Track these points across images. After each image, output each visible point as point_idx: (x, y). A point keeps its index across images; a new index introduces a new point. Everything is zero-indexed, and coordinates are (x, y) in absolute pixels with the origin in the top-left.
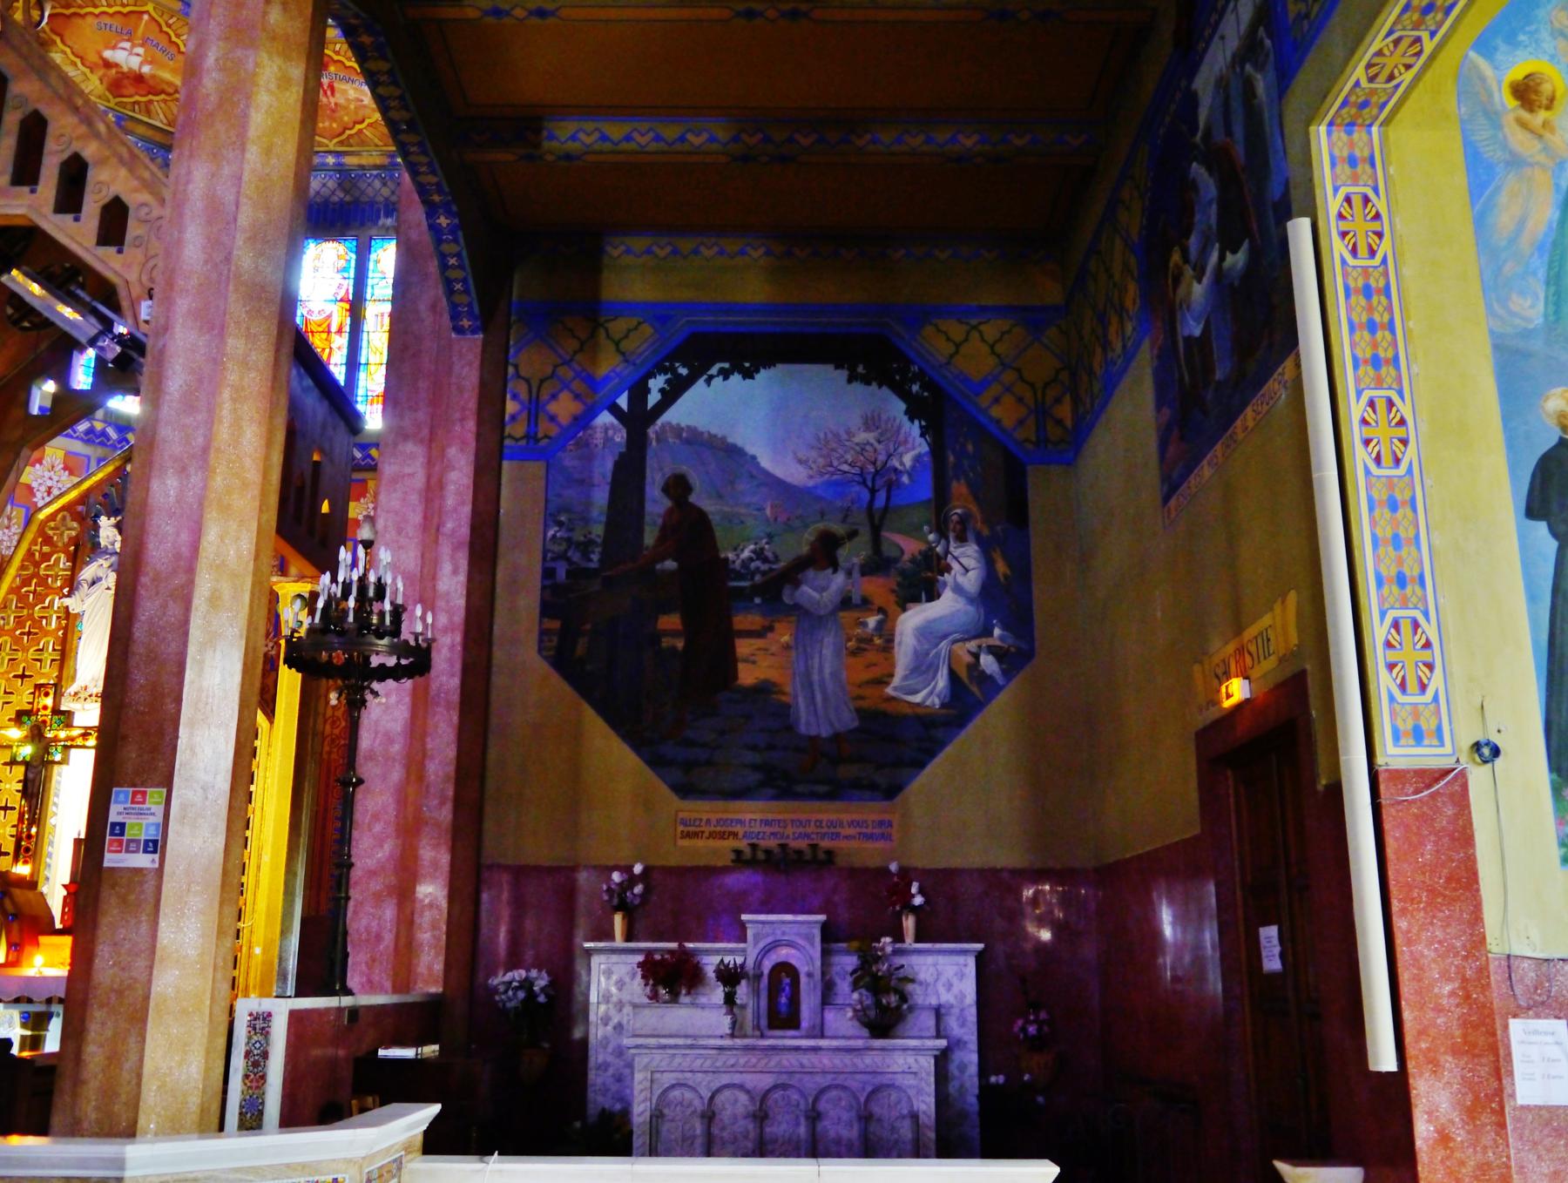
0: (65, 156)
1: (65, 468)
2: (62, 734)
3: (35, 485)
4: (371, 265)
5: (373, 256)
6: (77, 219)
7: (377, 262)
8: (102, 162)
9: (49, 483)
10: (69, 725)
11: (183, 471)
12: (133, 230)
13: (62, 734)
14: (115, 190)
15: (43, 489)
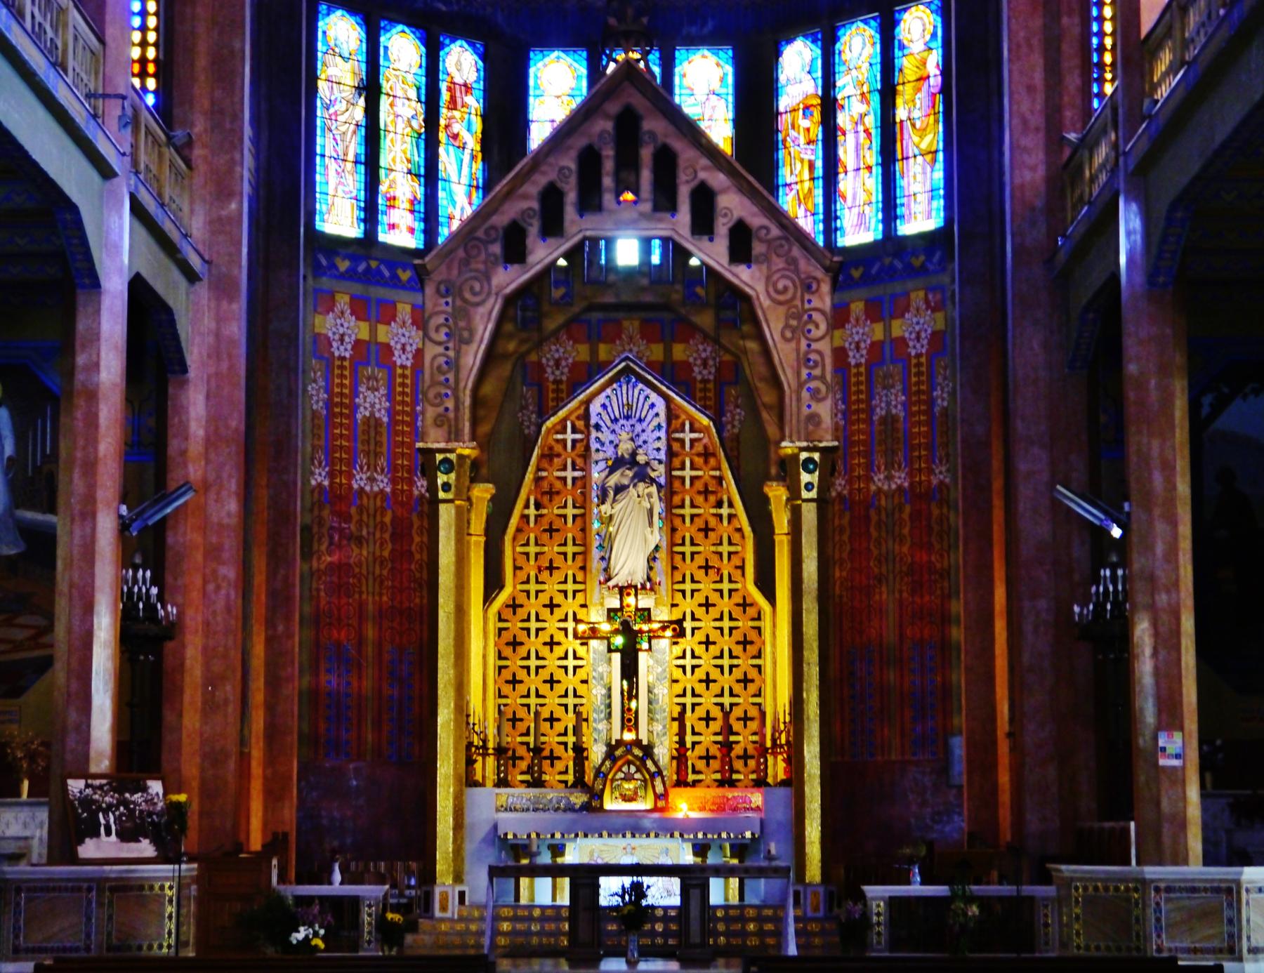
0: (695, 183)
1: (413, 324)
2: (645, 627)
3: (392, 343)
4: (677, 80)
5: (677, 70)
6: (711, 240)
7: (684, 75)
8: (725, 191)
9: (403, 340)
10: (649, 620)
11: (1168, 591)
12: (758, 248)
13: (645, 627)
14: (737, 214)
15: (399, 346)
